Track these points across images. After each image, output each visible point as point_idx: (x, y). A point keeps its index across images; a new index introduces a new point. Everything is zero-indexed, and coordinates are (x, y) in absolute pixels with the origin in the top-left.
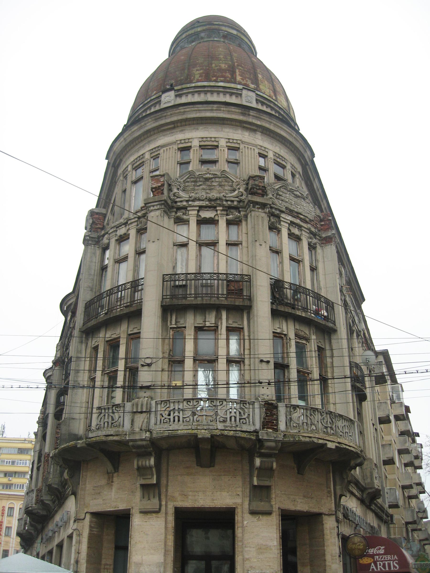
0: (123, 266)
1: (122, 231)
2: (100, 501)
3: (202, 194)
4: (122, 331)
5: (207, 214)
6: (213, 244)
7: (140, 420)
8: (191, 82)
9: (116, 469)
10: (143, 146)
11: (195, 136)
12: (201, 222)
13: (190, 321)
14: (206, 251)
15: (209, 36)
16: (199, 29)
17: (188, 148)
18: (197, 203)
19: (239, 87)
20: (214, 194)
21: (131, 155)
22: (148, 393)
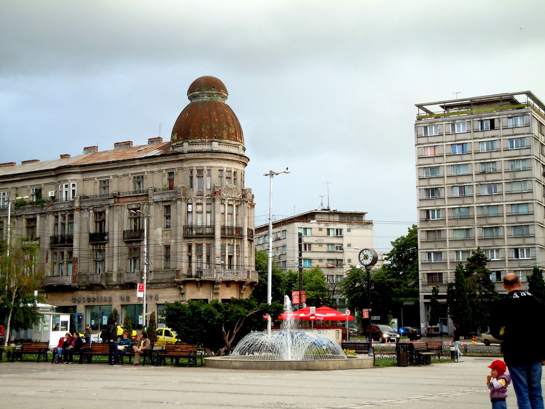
0: (199, 215)
1: (199, 201)
2: (195, 296)
3: (230, 196)
4: (204, 242)
5: (231, 203)
6: (232, 214)
7: (219, 275)
8: (223, 138)
9: (201, 286)
10: (203, 162)
11: (225, 165)
12: (229, 205)
13: (227, 242)
14: (230, 216)
15: (217, 96)
16: (214, 92)
17: (222, 170)
18: (229, 198)
19: (238, 143)
20: (233, 196)
21: (195, 162)
22: (219, 266)
